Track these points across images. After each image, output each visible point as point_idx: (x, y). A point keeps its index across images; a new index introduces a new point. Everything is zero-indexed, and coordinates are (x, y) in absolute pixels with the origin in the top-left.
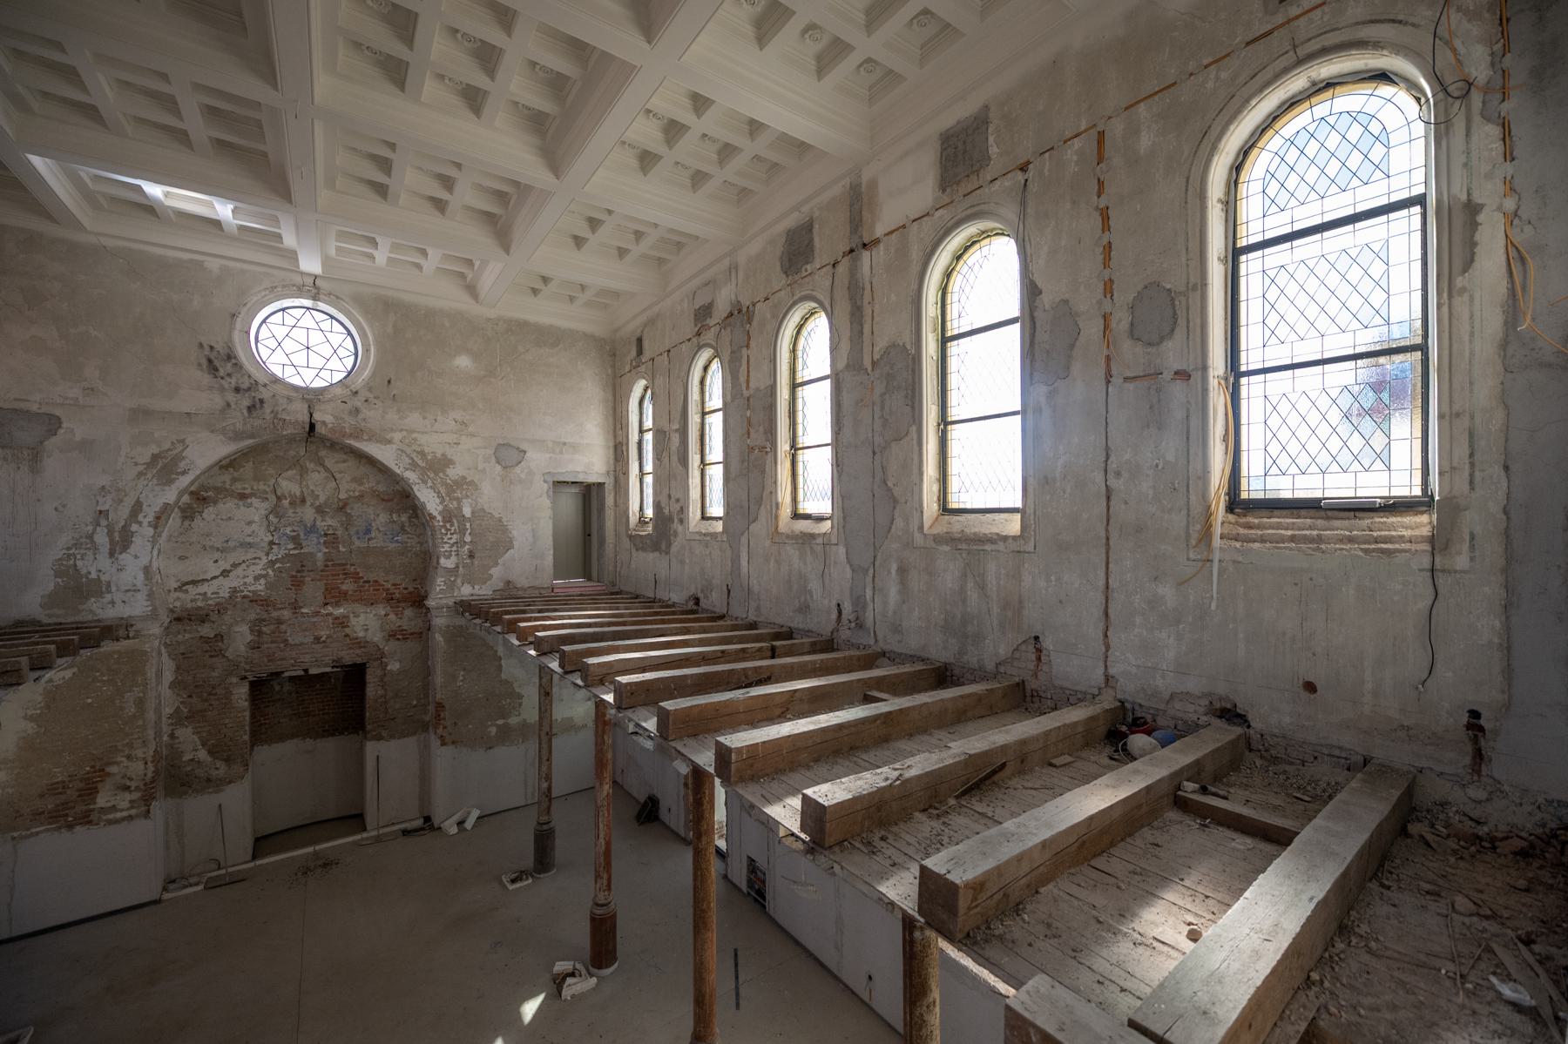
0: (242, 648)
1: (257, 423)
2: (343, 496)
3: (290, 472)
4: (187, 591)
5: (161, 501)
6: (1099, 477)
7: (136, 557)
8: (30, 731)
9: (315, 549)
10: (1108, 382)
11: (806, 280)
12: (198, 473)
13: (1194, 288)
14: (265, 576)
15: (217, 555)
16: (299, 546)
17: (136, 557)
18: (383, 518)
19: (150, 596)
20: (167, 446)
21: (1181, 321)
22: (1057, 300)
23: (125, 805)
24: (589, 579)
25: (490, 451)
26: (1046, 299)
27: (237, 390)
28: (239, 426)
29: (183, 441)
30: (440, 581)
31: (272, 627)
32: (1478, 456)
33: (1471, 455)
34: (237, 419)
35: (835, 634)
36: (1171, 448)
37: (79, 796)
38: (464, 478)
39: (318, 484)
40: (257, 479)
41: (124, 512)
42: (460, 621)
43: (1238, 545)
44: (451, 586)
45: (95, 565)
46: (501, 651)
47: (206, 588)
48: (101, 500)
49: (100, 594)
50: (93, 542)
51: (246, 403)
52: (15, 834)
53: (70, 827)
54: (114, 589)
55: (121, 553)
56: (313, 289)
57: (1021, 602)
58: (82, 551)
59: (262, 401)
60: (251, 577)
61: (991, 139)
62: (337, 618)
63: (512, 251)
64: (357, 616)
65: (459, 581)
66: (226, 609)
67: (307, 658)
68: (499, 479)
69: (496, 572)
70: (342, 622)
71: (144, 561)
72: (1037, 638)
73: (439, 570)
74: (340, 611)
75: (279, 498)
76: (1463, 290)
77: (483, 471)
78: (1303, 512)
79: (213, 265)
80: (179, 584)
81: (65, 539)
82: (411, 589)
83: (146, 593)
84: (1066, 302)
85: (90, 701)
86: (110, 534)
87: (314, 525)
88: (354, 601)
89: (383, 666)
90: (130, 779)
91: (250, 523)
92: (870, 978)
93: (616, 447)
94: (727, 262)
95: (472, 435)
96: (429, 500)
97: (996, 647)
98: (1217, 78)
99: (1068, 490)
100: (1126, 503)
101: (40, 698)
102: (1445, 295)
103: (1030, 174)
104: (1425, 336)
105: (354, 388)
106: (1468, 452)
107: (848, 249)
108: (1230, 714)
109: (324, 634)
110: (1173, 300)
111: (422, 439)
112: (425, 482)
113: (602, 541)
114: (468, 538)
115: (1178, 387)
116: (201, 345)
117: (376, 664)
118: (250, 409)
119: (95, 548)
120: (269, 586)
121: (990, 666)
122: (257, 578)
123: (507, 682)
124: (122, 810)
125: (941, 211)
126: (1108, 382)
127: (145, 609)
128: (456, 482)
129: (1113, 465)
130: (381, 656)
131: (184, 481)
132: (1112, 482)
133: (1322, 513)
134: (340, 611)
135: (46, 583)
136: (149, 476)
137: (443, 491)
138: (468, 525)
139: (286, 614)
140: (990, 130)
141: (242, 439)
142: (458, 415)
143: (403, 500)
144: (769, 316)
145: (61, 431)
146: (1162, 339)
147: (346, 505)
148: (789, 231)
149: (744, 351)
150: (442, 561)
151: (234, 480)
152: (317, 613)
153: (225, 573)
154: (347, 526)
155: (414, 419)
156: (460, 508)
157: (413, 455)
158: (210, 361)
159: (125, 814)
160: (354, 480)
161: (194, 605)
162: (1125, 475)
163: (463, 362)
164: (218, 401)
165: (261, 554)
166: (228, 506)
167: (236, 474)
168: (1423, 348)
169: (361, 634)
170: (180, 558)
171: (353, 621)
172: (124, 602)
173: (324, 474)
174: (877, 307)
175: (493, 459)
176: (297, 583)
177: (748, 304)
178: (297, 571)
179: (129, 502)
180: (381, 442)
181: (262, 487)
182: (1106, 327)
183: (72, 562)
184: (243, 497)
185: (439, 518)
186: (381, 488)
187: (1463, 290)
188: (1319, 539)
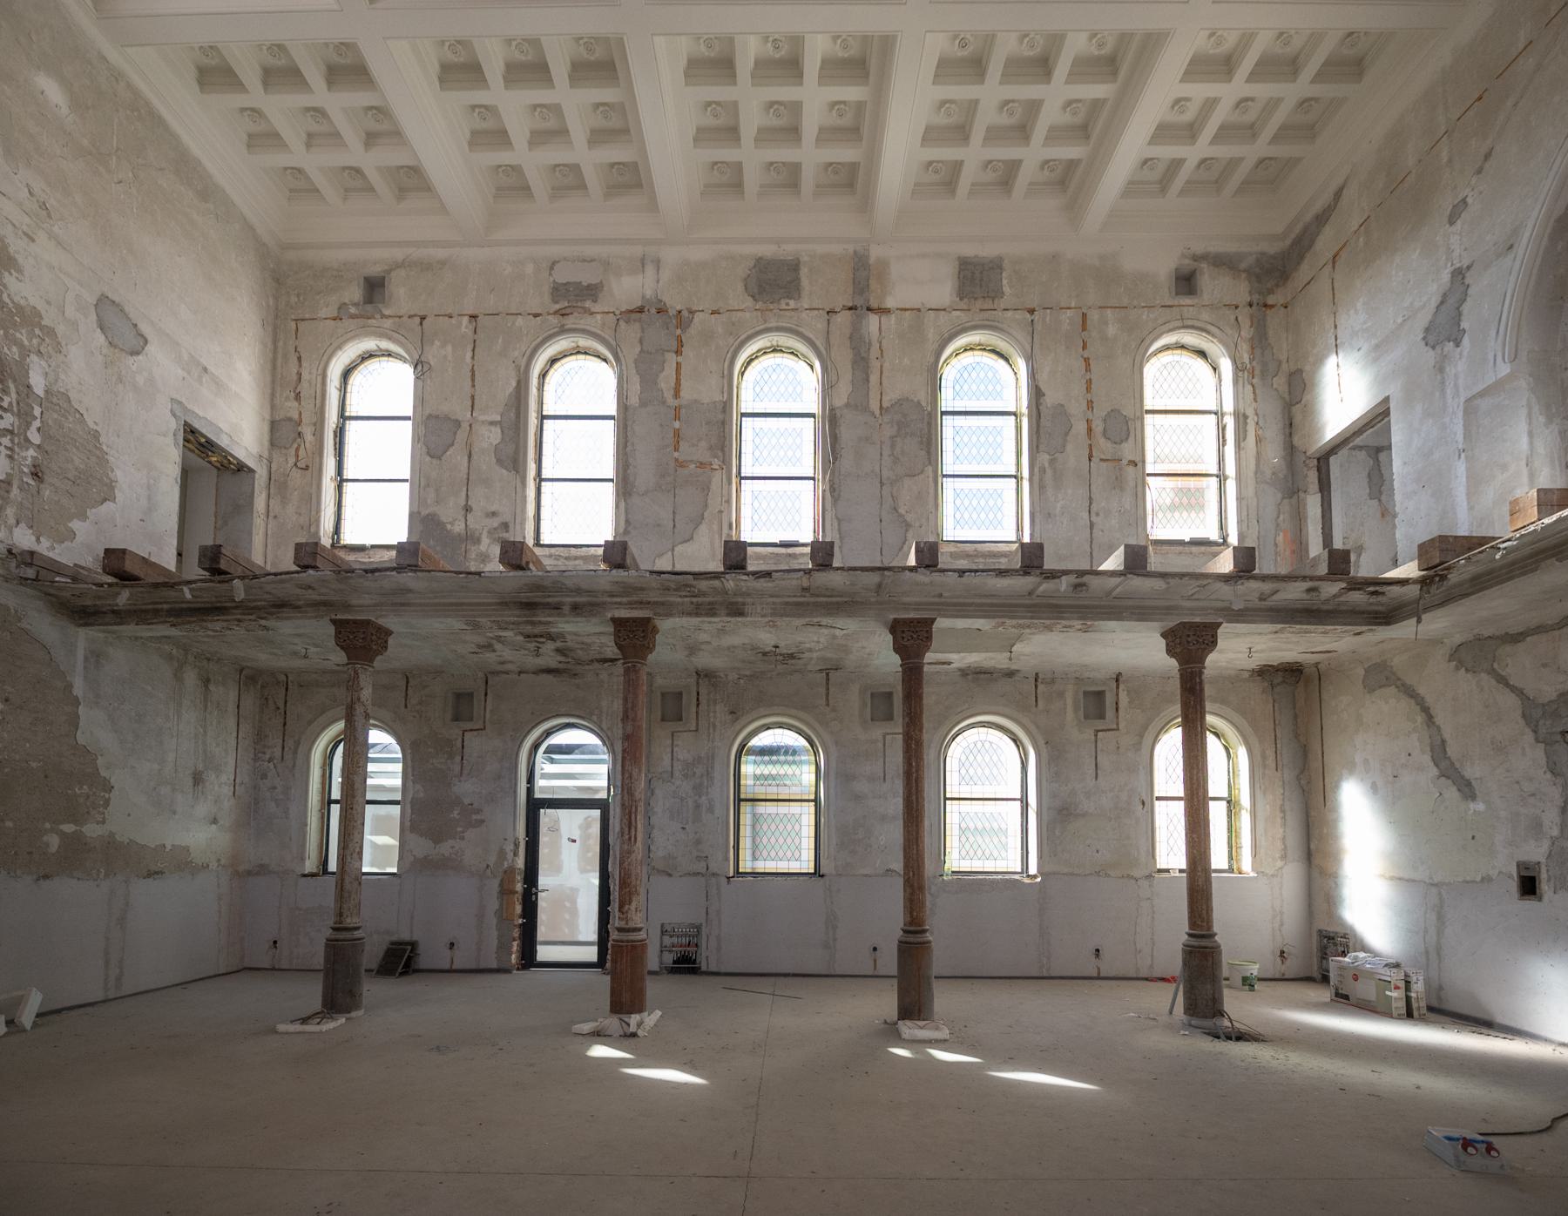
10: (1090, 460)
11: (787, 313)
21: (1132, 434)
46: (79, 689)
61: (1005, 282)
84: (1062, 406)
94: (638, 250)
98: (1148, 316)
99: (1065, 522)
100: (1102, 531)
103: (1036, 316)
107: (850, 304)
110: (1127, 422)
115: (1131, 469)
125: (958, 313)
129: (1094, 507)
132: (1094, 518)
138: (37, 411)
140: (1004, 275)
146: (1122, 441)
148: (761, 258)
149: (672, 358)
162: (1101, 514)
174: (886, 365)
177: (679, 308)
187: (1243, 449)
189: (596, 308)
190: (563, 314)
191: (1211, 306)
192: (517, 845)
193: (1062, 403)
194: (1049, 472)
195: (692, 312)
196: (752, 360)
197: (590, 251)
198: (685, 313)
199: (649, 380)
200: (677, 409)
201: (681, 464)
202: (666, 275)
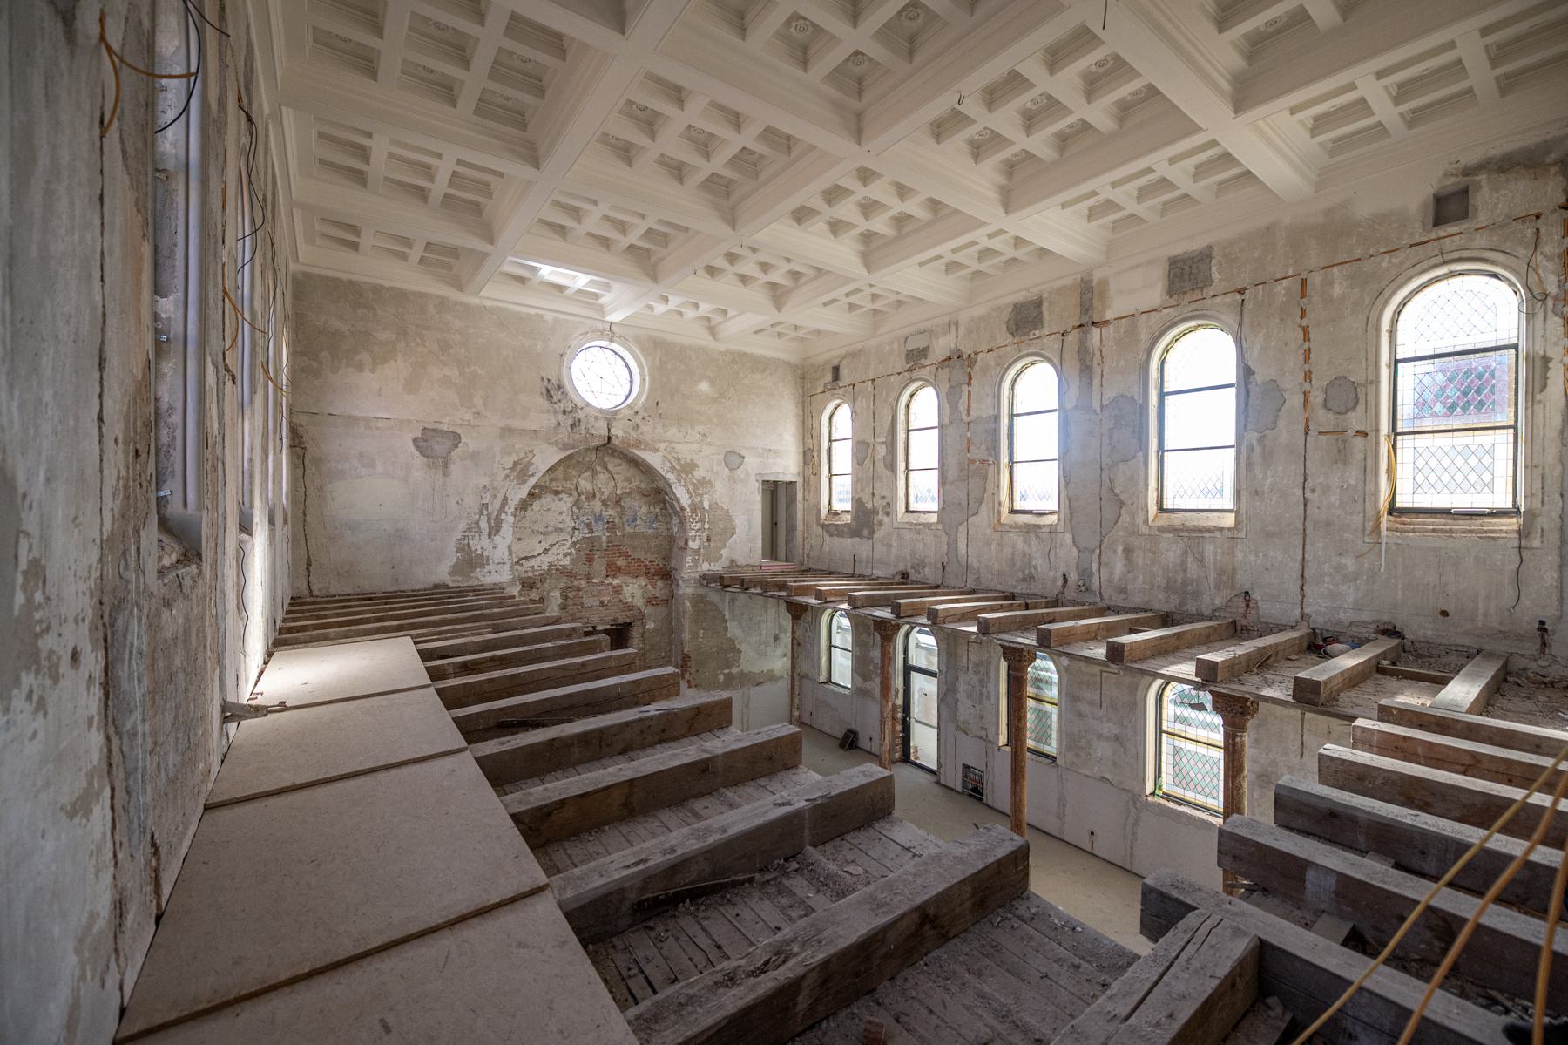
0: (556, 609)
1: (577, 436)
2: (619, 492)
3: (587, 474)
4: (522, 565)
6: (1299, 492)
7: (504, 538)
9: (600, 531)
10: (1306, 434)
12: (541, 474)
13: (1371, 382)
14: (570, 554)
15: (541, 537)
16: (591, 531)
17: (504, 538)
18: (644, 510)
20: (522, 455)
21: (1362, 401)
22: (1268, 379)
24: (776, 560)
25: (721, 457)
26: (1259, 378)
27: (564, 412)
28: (566, 439)
29: (531, 451)
30: (689, 559)
31: (574, 593)
32: (1546, 488)
33: (1543, 488)
34: (564, 433)
35: (1060, 596)
36: (1353, 476)
38: (704, 478)
39: (603, 483)
40: (565, 479)
41: (497, 504)
42: (702, 591)
43: (1398, 534)
44: (696, 562)
45: (480, 544)
47: (532, 563)
49: (482, 566)
51: (570, 422)
56: (610, 333)
57: (1234, 569)
59: (579, 420)
60: (560, 554)
62: (614, 587)
63: (784, 310)
64: (627, 586)
65: (701, 560)
66: (545, 579)
67: (595, 618)
68: (727, 479)
69: (723, 552)
70: (617, 591)
71: (509, 541)
72: (1247, 593)
73: (689, 552)
74: (616, 582)
75: (579, 494)
76: (1540, 402)
77: (717, 473)
78: (1439, 516)
79: (549, 316)
81: (462, 525)
82: (661, 565)
84: (1275, 381)
87: (601, 515)
88: (625, 574)
89: (644, 625)
91: (561, 513)
92: (1092, 833)
93: (804, 453)
95: (710, 444)
96: (682, 495)
97: (1213, 599)
99: (1274, 499)
100: (1319, 508)
102: (1530, 403)
104: (1516, 421)
105: (636, 409)
106: (1540, 486)
108: (1391, 632)
109: (606, 599)
111: (678, 447)
112: (679, 482)
113: (791, 529)
114: (707, 526)
115: (1359, 441)
116: (542, 379)
117: (639, 623)
118: (573, 426)
120: (572, 561)
121: (1207, 612)
122: (565, 555)
123: (730, 640)
126: (1306, 434)
128: (699, 481)
129: (1309, 484)
130: (642, 617)
131: (532, 481)
133: (1451, 516)
134: (616, 582)
135: (452, 557)
137: (691, 488)
139: (583, 583)
141: (567, 449)
142: (700, 428)
143: (659, 495)
144: (993, 363)
145: (460, 445)
146: (1347, 411)
147: (620, 499)
150: (690, 543)
151: (552, 480)
152: (602, 583)
153: (546, 551)
154: (621, 514)
155: (673, 432)
156: (701, 502)
157: (673, 460)
158: (548, 390)
160: (628, 480)
161: (526, 575)
162: (1318, 491)
163: (704, 386)
164: (555, 422)
165: (568, 537)
166: (548, 499)
167: (553, 475)
168: (1515, 428)
169: (630, 600)
171: (625, 589)
173: (607, 475)
175: (723, 464)
176: (590, 560)
178: (589, 550)
179: (500, 497)
180: (651, 450)
181: (569, 485)
182: (1306, 401)
184: (557, 493)
185: (688, 510)
186: (643, 486)
188: (1451, 531)
189: (927, 362)
190: (911, 370)
191: (1491, 227)
192: (897, 692)
193: (1275, 378)
194: (1258, 450)
195: (976, 354)
196: (1018, 376)
197: (923, 326)
198: (972, 355)
199: (954, 407)
200: (969, 423)
201: (973, 461)
202: (962, 331)
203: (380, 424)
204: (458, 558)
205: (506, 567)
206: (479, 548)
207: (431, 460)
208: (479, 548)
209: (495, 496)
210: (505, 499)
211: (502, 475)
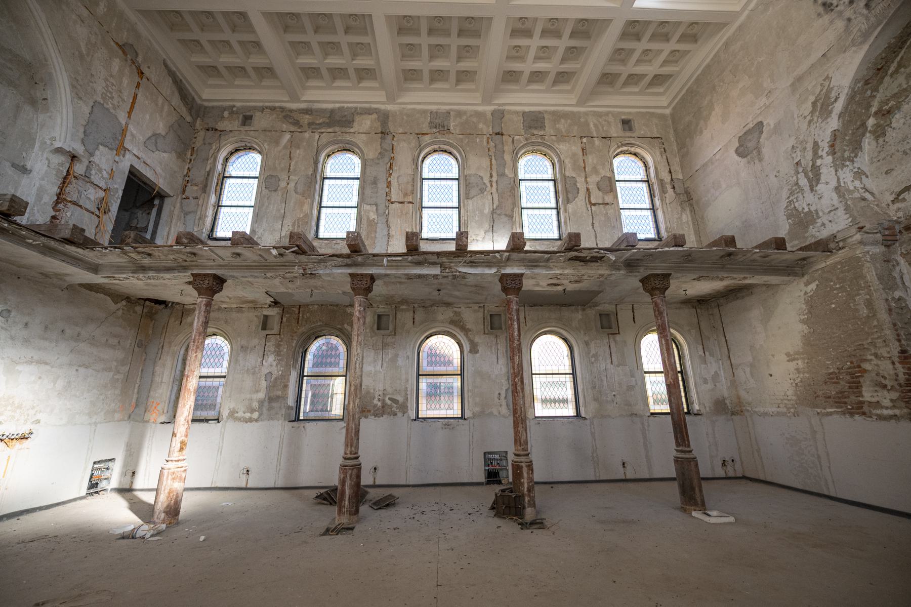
4: (904, 200)
5: (828, 133)
8: (806, 331)
17: (827, 183)
19: (847, 209)
23: (886, 402)
37: (850, 387)
41: (809, 155)
48: (794, 155)
49: (814, 222)
50: (799, 186)
52: (819, 410)
53: (852, 414)
54: (821, 214)
55: (817, 186)
58: (796, 196)
71: (834, 183)
80: (894, 196)
81: (785, 194)
83: (843, 208)
85: (833, 306)
86: (806, 176)
90: (885, 378)
101: (804, 307)
119: (802, 190)
124: (887, 408)
127: (847, 222)
131: (839, 106)
136: (815, 119)
159: (890, 412)
170: (886, 173)
172: (830, 221)
179: (810, 146)
183: (792, 206)
203: (718, 157)
204: (790, 225)
205: (841, 212)
206: (805, 206)
207: (749, 157)
208: (805, 206)
209: (805, 149)
210: (816, 145)
211: (805, 125)
